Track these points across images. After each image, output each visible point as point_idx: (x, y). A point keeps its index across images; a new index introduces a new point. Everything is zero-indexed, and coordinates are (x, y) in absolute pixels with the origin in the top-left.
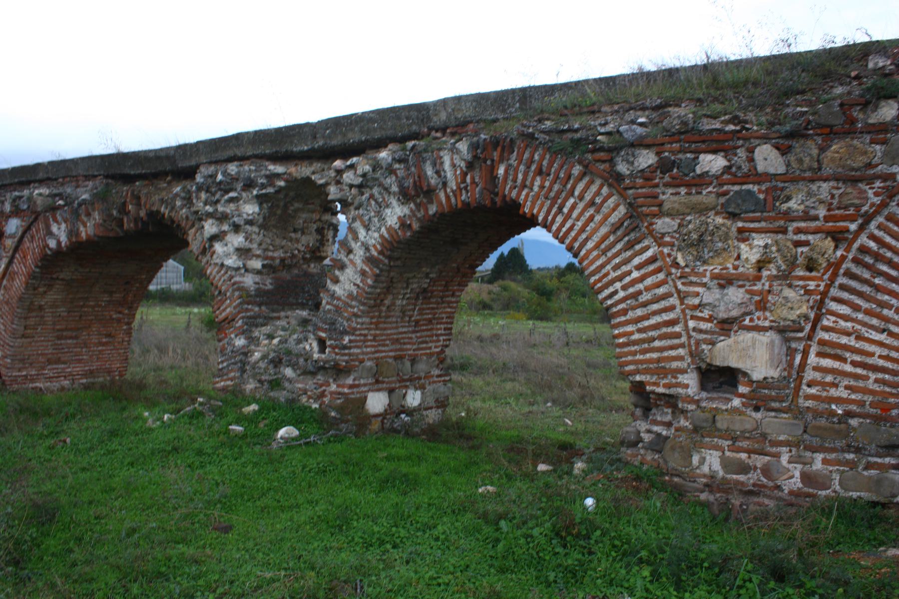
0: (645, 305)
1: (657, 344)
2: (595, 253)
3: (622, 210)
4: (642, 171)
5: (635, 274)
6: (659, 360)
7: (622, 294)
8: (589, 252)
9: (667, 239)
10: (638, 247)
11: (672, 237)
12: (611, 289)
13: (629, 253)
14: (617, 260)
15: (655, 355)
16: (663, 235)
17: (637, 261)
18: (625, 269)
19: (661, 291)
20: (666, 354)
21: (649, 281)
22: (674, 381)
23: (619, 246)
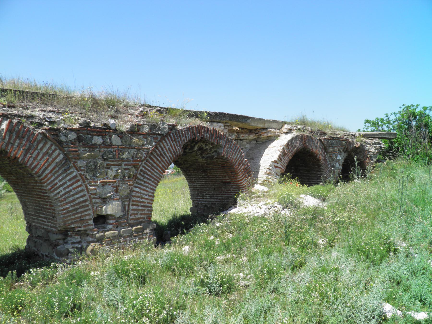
0: (73, 195)
1: (79, 210)
2: (50, 175)
3: (62, 156)
4: (71, 141)
5: (69, 183)
6: (80, 217)
7: (63, 192)
8: (47, 175)
9: (82, 168)
10: (68, 172)
11: (84, 168)
12: (58, 191)
13: (65, 175)
14: (60, 178)
15: (79, 215)
16: (81, 167)
17: (68, 178)
18: (64, 181)
19: (80, 189)
20: (83, 214)
21: (74, 186)
22: (87, 224)
23: (60, 172)
